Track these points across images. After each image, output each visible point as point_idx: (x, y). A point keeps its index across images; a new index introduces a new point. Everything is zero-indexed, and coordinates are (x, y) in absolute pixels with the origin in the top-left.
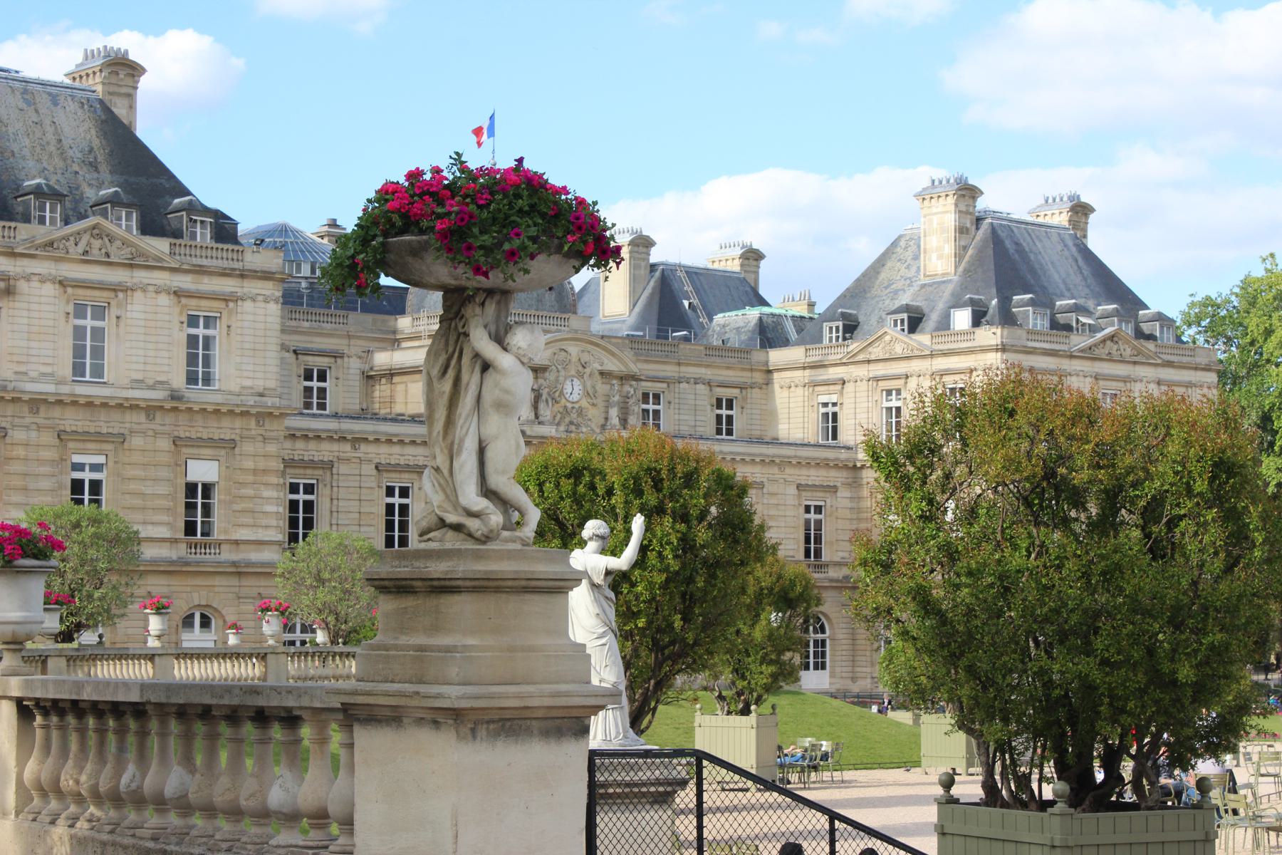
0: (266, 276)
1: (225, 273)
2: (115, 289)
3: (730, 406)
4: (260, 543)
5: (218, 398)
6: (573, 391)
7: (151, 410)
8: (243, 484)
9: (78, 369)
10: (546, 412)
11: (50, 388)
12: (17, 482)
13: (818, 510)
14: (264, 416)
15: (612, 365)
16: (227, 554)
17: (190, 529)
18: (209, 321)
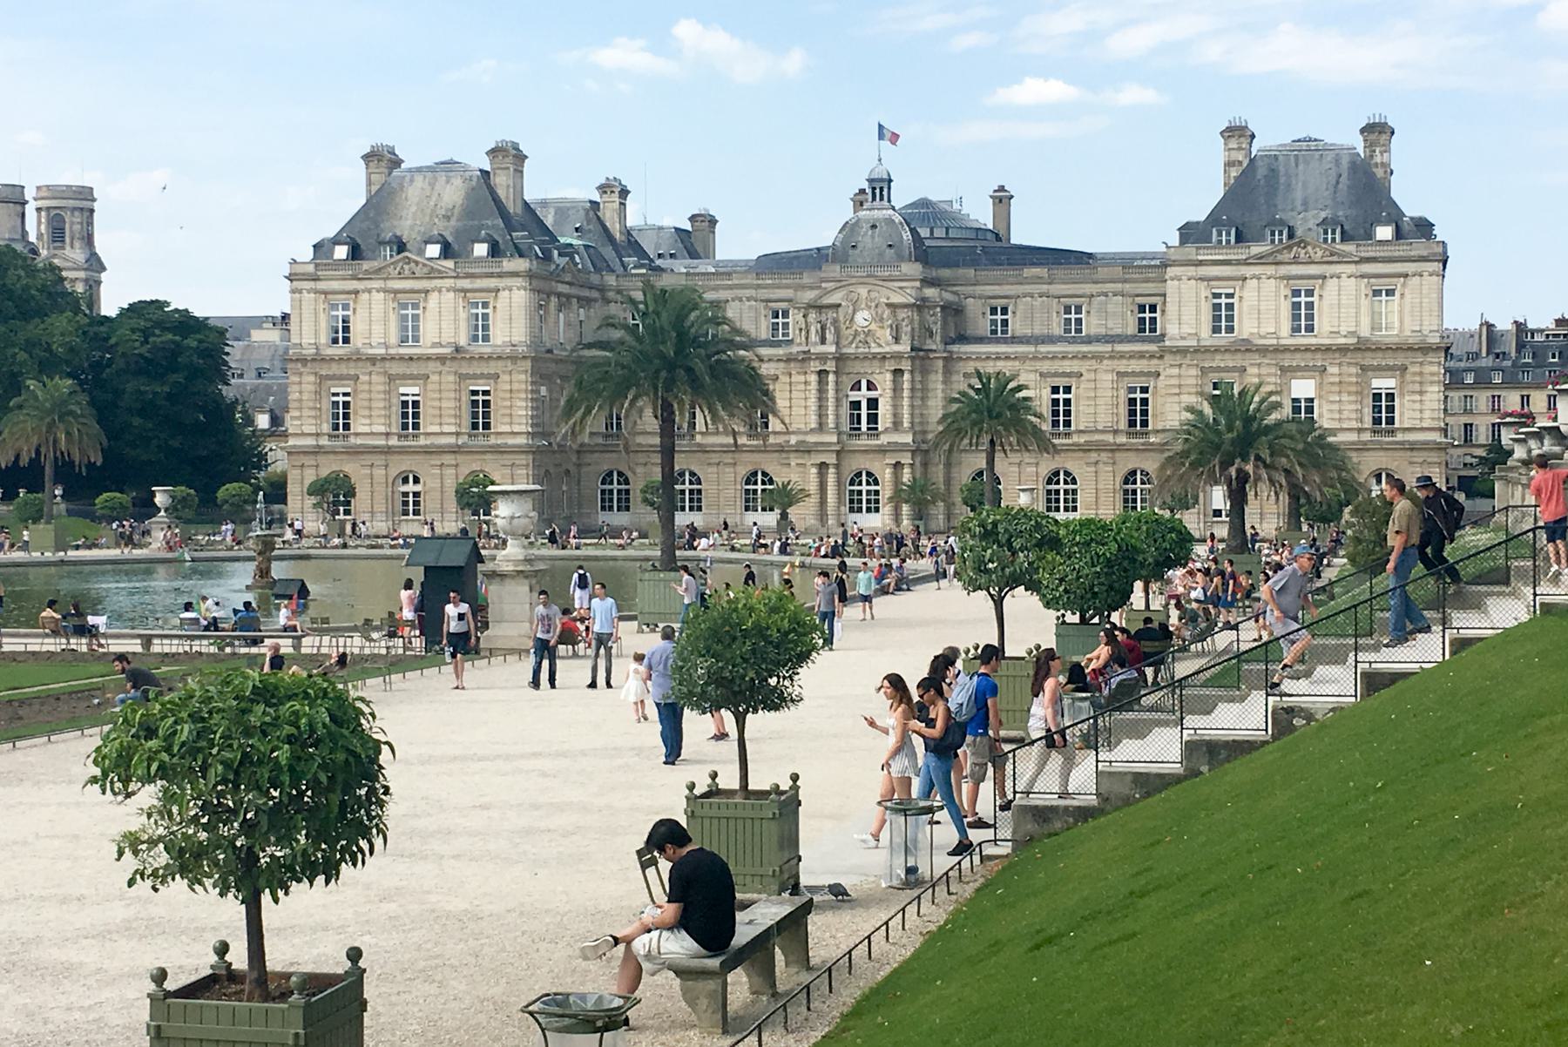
0: (515, 274)
1: (491, 275)
2: (418, 292)
3: (1153, 309)
4: (513, 433)
5: (488, 350)
6: (862, 318)
7: (442, 359)
8: (504, 399)
9: (404, 340)
10: (829, 337)
11: (383, 351)
12: (366, 404)
13: (1145, 390)
14: (513, 358)
15: (897, 299)
16: (493, 440)
17: (475, 426)
18: (485, 305)
